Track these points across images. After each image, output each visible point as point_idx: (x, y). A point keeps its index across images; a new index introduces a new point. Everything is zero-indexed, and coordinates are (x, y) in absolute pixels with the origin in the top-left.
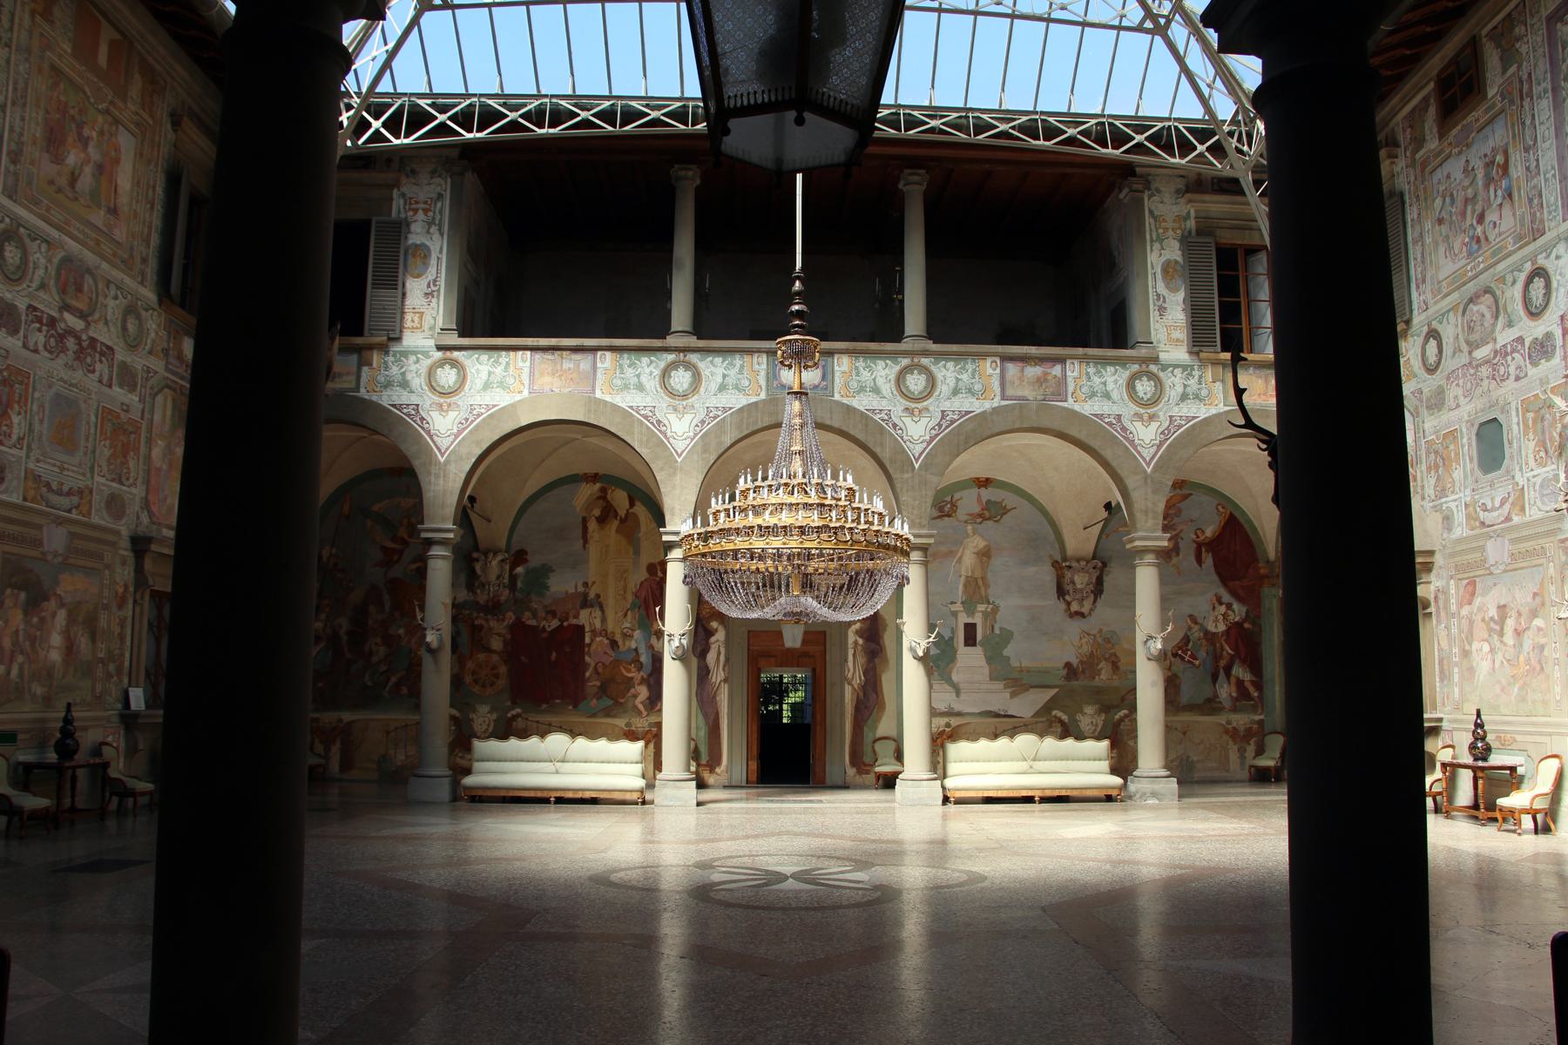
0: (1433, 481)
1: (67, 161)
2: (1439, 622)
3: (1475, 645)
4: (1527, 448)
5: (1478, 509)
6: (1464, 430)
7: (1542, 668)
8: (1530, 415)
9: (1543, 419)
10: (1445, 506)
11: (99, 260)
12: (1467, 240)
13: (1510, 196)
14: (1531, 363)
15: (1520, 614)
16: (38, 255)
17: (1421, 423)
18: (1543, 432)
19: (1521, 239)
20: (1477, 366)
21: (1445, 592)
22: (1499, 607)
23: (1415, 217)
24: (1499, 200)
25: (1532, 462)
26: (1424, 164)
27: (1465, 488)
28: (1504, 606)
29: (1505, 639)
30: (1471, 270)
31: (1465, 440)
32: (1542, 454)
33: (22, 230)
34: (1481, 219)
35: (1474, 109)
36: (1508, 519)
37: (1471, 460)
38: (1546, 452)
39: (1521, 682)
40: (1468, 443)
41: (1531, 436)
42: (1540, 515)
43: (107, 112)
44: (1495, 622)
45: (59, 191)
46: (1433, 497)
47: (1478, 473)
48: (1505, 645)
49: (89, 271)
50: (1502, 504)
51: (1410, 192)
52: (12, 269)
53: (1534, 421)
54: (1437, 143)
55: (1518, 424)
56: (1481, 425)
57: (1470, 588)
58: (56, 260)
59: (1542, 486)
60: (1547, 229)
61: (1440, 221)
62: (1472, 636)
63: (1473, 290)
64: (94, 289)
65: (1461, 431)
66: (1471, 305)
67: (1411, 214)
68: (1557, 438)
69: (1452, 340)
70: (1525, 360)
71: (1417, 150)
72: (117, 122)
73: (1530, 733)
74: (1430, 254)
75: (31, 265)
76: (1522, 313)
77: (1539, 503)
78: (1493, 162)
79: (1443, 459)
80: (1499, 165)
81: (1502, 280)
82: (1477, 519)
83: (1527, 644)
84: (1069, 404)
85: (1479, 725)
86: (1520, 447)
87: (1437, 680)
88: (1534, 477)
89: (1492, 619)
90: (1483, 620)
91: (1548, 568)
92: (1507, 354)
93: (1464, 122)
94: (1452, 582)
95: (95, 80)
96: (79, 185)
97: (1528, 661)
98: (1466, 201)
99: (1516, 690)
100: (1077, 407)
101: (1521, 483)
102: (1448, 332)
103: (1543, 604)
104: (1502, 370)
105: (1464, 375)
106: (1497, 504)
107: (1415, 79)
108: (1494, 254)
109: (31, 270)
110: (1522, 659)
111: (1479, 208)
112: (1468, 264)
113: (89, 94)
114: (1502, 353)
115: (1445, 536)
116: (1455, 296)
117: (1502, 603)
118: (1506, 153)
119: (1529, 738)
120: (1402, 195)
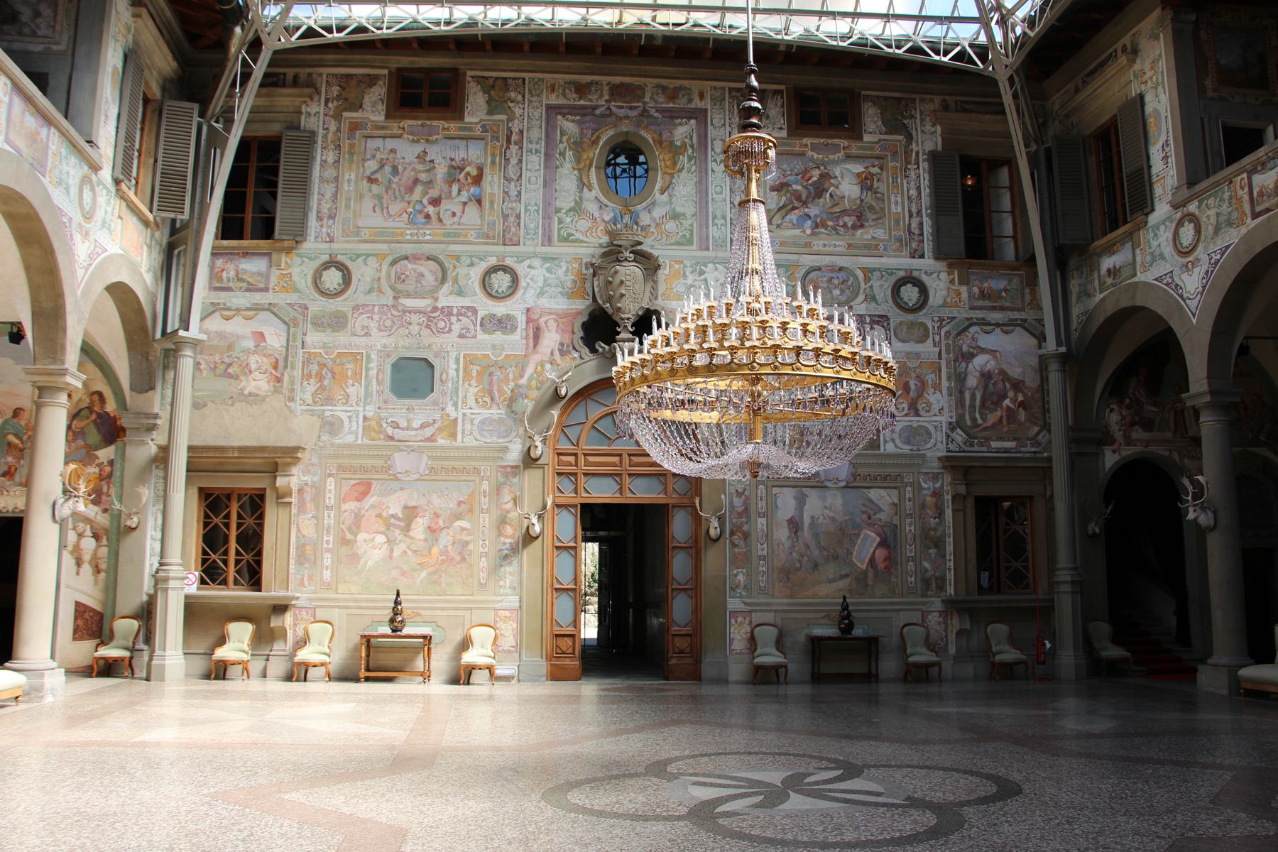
0: (311, 387)
2: (302, 508)
3: (361, 537)
4: (467, 391)
5: (385, 425)
6: (374, 356)
7: (464, 559)
8: (475, 369)
9: (491, 374)
10: (327, 414)
12: (410, 210)
13: (479, 202)
14: (483, 330)
15: (437, 515)
17: (300, 336)
18: (491, 384)
19: (488, 237)
20: (404, 312)
21: (319, 490)
22: (406, 507)
23: (331, 160)
24: (464, 199)
25: (471, 402)
26: (354, 127)
27: (366, 404)
28: (415, 508)
29: (411, 534)
30: (411, 235)
31: (373, 365)
32: (488, 400)
34: (436, 202)
35: (444, 119)
36: (431, 439)
37: (379, 383)
38: (492, 399)
39: (432, 569)
40: (378, 372)
41: (473, 382)
42: (477, 444)
44: (399, 519)
46: (310, 402)
47: (392, 397)
48: (411, 538)
50: (423, 426)
51: (325, 136)
53: (478, 373)
54: (382, 118)
55: (457, 370)
56: (401, 359)
57: (362, 489)
59: (483, 422)
60: (521, 243)
61: (371, 180)
62: (358, 526)
63: (409, 252)
65: (368, 357)
66: (406, 262)
67: (323, 157)
68: (509, 392)
69: (368, 279)
70: (475, 325)
71: (346, 110)
73: (442, 609)
74: (348, 200)
76: (478, 290)
77: (476, 434)
78: (462, 169)
79: (333, 373)
80: (468, 174)
81: (458, 258)
82: (383, 431)
83: (445, 539)
84: (46, 181)
85: (397, 603)
86: (457, 390)
87: (292, 562)
88: (472, 414)
89: (393, 516)
90: (379, 516)
91: (481, 484)
92: (450, 314)
93: (428, 123)
94: (331, 479)
97: (444, 552)
98: (416, 181)
99: (424, 574)
100: (51, 189)
101: (453, 415)
102: (363, 273)
103: (470, 511)
104: (442, 325)
105: (379, 313)
106: (416, 424)
107: (369, 57)
108: (448, 235)
110: (435, 550)
111: (434, 193)
112: (409, 229)
114: (448, 312)
115: (323, 438)
116: (385, 246)
117: (413, 504)
118: (481, 170)
119: (438, 612)
120: (313, 134)
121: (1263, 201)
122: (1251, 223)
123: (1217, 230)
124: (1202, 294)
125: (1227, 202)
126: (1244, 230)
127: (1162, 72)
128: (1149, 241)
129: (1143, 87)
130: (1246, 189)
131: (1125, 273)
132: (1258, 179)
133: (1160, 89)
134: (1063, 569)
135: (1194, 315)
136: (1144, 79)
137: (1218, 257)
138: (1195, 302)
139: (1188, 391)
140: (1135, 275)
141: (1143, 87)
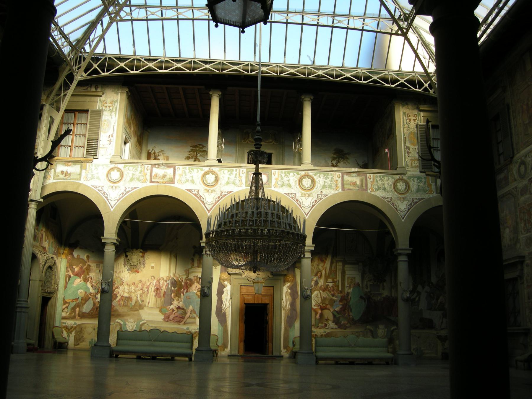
121: (156, 178)
122: (148, 184)
123: (132, 180)
124: (118, 201)
125: (139, 172)
126: (145, 185)
127: (116, 108)
128: (91, 169)
129: (104, 108)
130: (149, 171)
131: (72, 177)
132: (156, 170)
133: (113, 114)
134: (24, 301)
135: (112, 207)
136: (106, 105)
137: (130, 190)
138: (114, 203)
139: (103, 236)
140: (80, 180)
141: (104, 108)
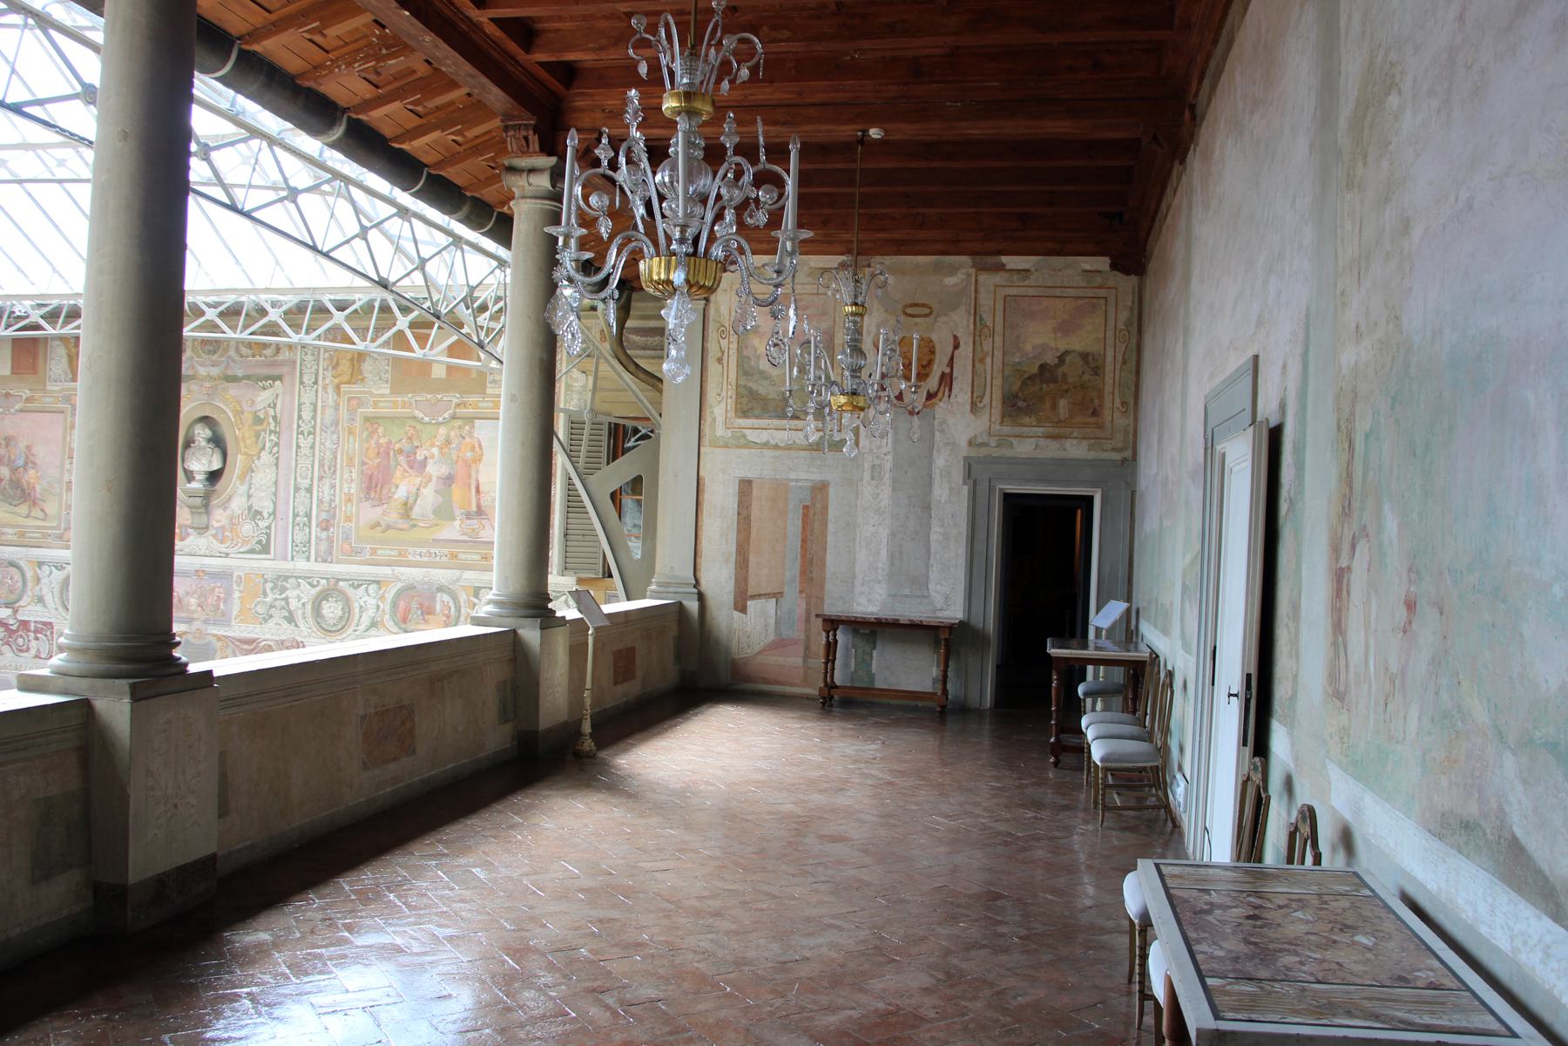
1: (396, 497)
11: (457, 573)
16: (359, 597)
33: (341, 583)
43: (454, 417)
45: (389, 527)
49: (441, 589)
52: (331, 622)
58: (390, 596)
64: (452, 604)
72: (470, 420)
75: (357, 610)
95: (429, 396)
96: (416, 512)
109: (357, 616)
113: (421, 415)
